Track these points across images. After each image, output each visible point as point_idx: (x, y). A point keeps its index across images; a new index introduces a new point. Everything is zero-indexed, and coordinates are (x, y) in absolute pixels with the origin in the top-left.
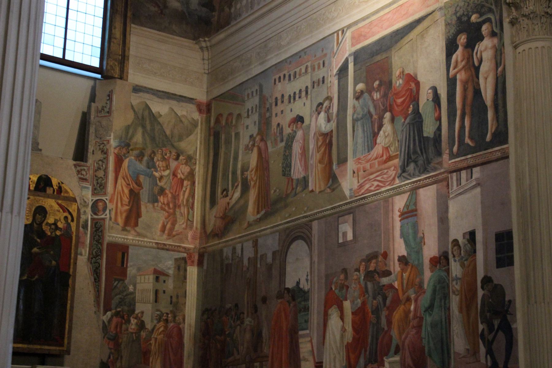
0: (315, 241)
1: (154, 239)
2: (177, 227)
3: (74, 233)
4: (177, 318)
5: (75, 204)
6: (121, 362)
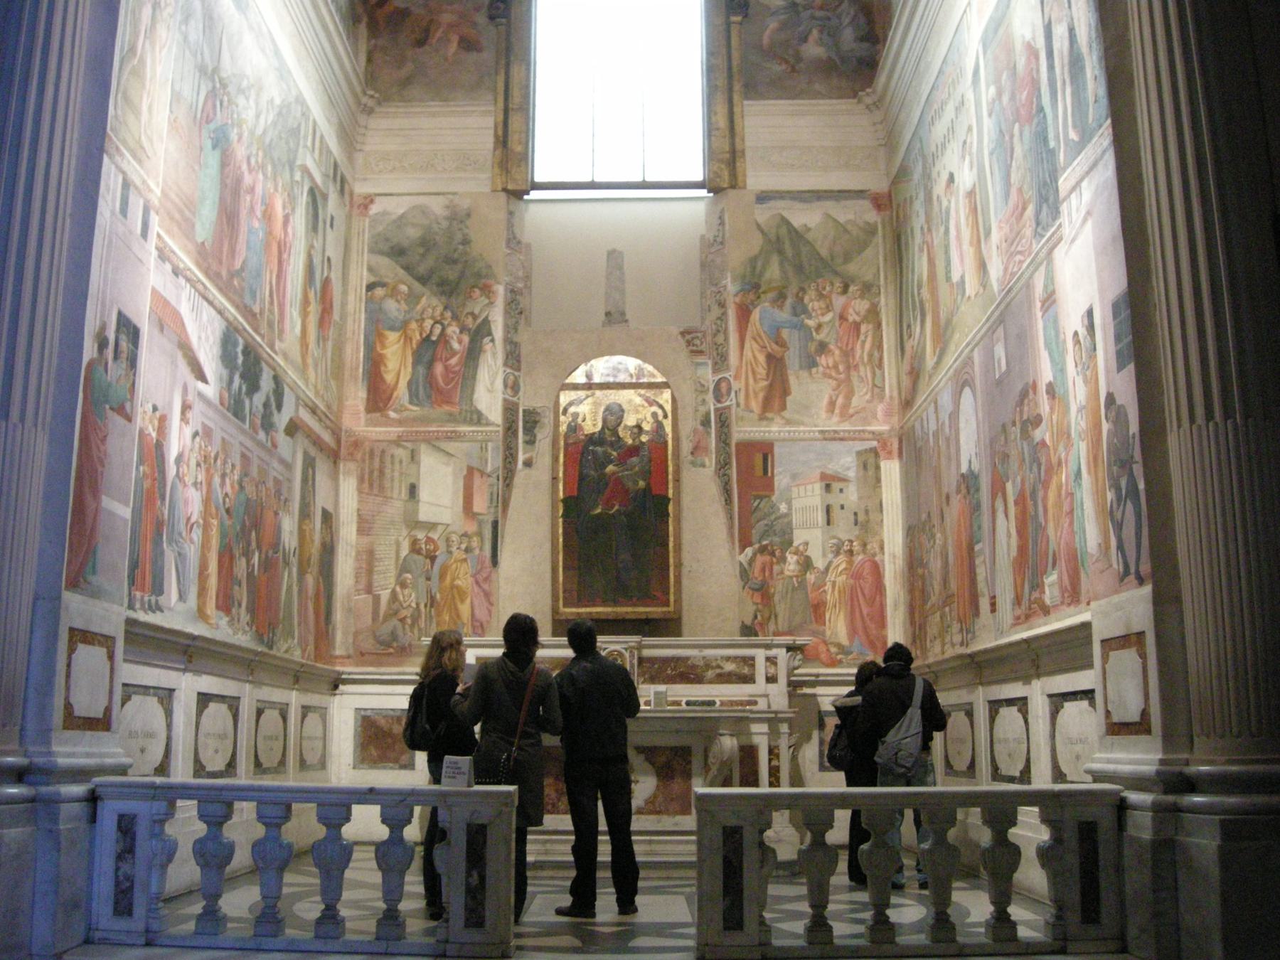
0: (978, 382)
1: (816, 426)
2: (855, 401)
3: (670, 436)
4: (869, 547)
6: (776, 623)
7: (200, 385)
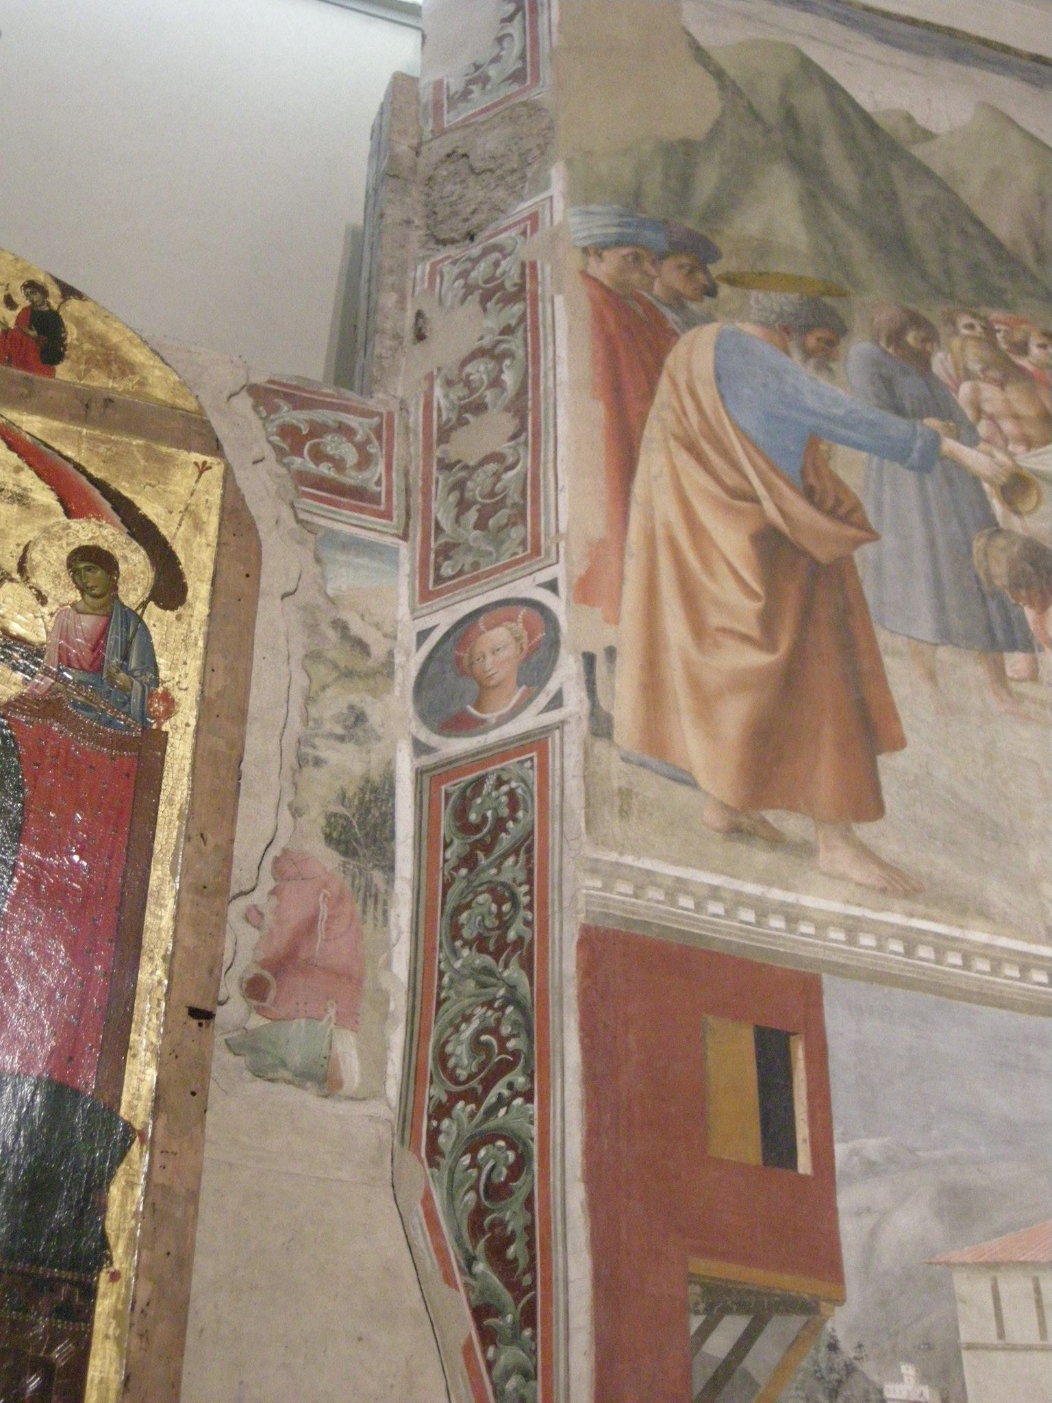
5: (203, 468)
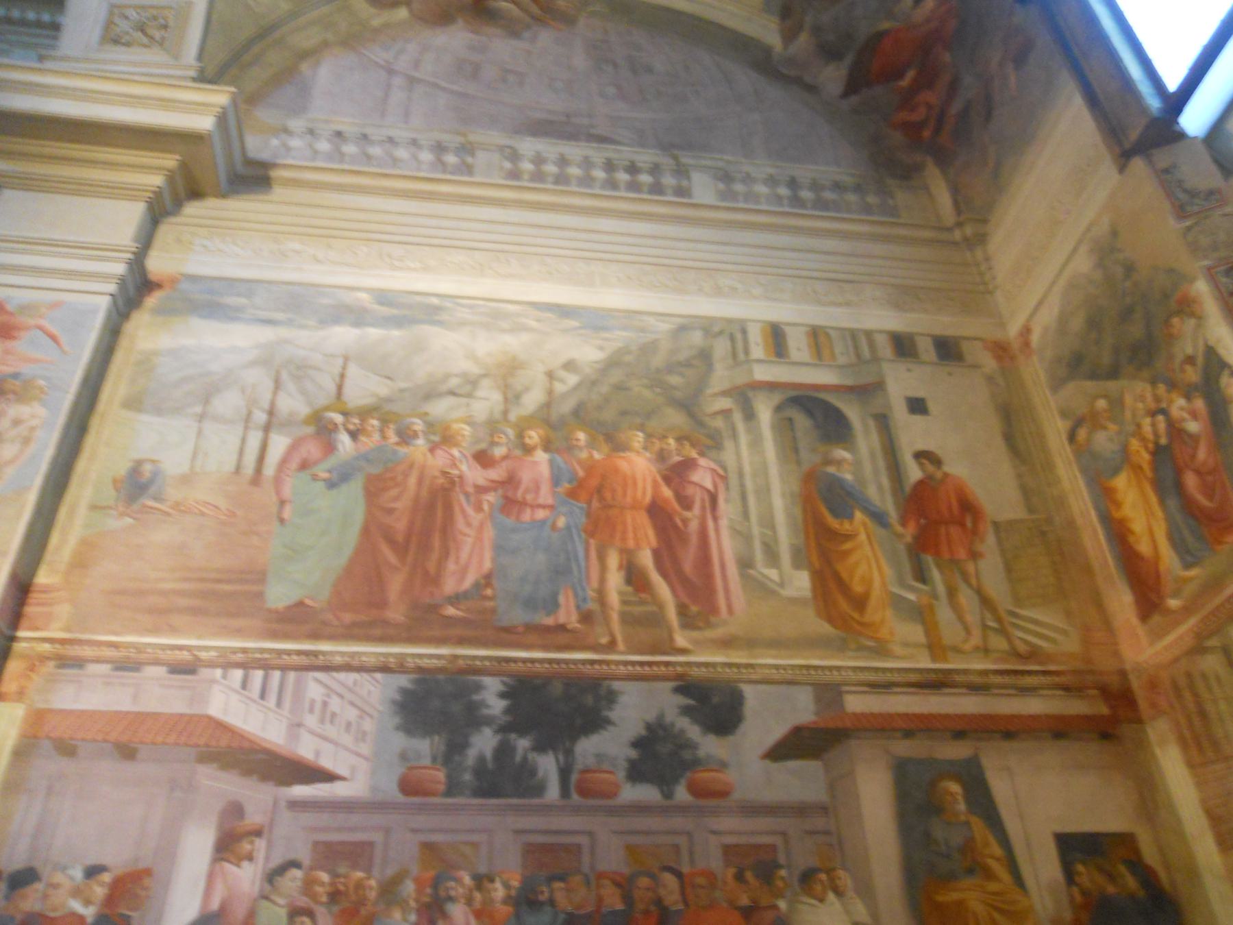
7: (301, 791)
